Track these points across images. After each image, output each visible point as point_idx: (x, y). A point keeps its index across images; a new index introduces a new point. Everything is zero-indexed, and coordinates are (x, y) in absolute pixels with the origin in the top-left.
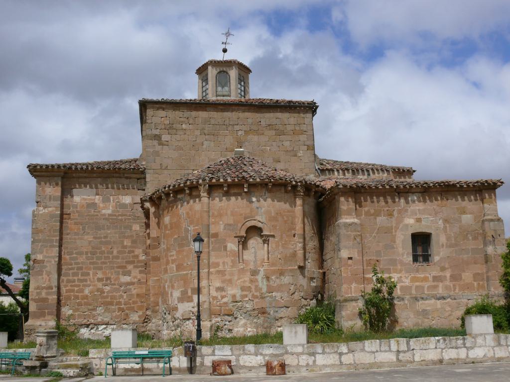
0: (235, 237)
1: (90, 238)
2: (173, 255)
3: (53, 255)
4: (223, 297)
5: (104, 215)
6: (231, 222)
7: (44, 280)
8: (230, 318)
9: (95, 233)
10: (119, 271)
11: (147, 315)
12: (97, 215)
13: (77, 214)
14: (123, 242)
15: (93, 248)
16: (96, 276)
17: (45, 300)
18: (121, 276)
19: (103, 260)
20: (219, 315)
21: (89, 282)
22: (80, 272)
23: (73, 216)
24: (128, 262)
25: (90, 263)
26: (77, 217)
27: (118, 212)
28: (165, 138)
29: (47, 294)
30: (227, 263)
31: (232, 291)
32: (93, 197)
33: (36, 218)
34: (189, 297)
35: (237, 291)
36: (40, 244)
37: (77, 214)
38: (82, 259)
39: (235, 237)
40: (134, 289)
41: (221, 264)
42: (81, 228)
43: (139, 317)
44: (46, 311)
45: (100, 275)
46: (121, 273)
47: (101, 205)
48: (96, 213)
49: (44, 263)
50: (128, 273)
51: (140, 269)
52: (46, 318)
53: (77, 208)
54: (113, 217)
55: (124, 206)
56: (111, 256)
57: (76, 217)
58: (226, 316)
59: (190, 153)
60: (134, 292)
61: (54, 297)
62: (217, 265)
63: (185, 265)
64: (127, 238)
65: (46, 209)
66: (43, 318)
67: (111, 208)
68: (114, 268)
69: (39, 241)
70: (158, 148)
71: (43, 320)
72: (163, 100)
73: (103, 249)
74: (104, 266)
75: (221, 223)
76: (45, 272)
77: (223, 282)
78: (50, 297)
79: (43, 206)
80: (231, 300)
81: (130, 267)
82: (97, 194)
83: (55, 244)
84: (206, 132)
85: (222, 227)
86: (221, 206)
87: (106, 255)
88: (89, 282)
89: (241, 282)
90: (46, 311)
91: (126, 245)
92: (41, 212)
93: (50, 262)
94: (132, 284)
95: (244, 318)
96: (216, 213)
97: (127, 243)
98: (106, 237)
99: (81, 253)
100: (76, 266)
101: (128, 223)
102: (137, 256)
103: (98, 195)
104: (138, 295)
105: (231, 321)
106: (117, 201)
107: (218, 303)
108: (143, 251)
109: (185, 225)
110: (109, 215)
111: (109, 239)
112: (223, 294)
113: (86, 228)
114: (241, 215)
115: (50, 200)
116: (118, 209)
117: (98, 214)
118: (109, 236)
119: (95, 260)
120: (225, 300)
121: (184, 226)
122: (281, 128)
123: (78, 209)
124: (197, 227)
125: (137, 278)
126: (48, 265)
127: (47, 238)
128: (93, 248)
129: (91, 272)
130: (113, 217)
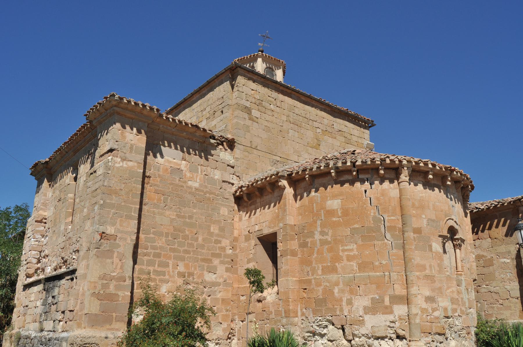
0: (440, 236)
1: (171, 214)
2: (352, 250)
3: (129, 229)
4: (434, 310)
5: (190, 187)
6: (434, 218)
7: (114, 267)
8: (441, 338)
9: (178, 210)
10: (204, 265)
11: (232, 329)
12: (182, 186)
13: (159, 179)
14: (209, 226)
15: (175, 229)
16: (177, 269)
17: (111, 297)
18: (205, 273)
19: (186, 248)
20: (430, 333)
21: (167, 277)
22: (157, 260)
23: (153, 180)
24: (214, 255)
25: (171, 249)
26: (158, 183)
27: (206, 187)
28: (255, 113)
29: (117, 287)
30: (434, 266)
31: (444, 303)
32: (179, 162)
33: (110, 172)
34: (386, 307)
35: (448, 304)
36: (113, 211)
37: (159, 179)
38: (161, 242)
39: (440, 236)
40: (220, 292)
41: (428, 267)
42: (162, 198)
43: (224, 330)
44: (114, 314)
45: (181, 268)
46: (206, 268)
47: (188, 175)
48: (181, 184)
49: (115, 240)
50: (212, 270)
51: (227, 265)
52: (113, 326)
53: (158, 170)
54: (200, 193)
55: (212, 181)
56: (195, 244)
57: (156, 183)
58: (437, 335)
59: (277, 138)
60: (219, 296)
61: (126, 293)
62: (423, 268)
63: (377, 263)
64: (214, 223)
65: (125, 162)
66: (108, 326)
67: (198, 181)
68: (198, 261)
69: (112, 206)
70: (249, 123)
71: (108, 329)
72: (259, 72)
73: (187, 233)
74: (187, 256)
75: (424, 216)
76: (115, 254)
77: (433, 290)
78: (120, 293)
79: (121, 157)
80: (444, 315)
81: (216, 262)
82: (184, 159)
83: (133, 214)
84: (291, 120)
85: (425, 222)
86: (422, 197)
87: (190, 242)
88: (167, 277)
89: (450, 292)
90: (114, 314)
91: (213, 233)
92: (117, 165)
93: (125, 239)
94: (218, 284)
95: (454, 339)
96: (417, 204)
97: (214, 230)
98: (190, 217)
99: (160, 234)
100: (153, 251)
101: (216, 203)
102: (223, 249)
103: (185, 160)
104: (223, 300)
105: (442, 342)
106: (205, 173)
107: (429, 317)
108: (231, 242)
109: (375, 213)
110: (196, 189)
111: (194, 220)
112: (435, 305)
113: (169, 201)
114: (442, 211)
115: (131, 152)
116: (206, 184)
117: (183, 184)
118: (195, 216)
119: (176, 246)
120: (436, 314)
121: (372, 214)
122: (349, 137)
123: (161, 173)
124: (392, 218)
125: (223, 278)
126: (121, 244)
127: (123, 204)
128: (175, 229)
129: (171, 263)
130: (200, 193)
